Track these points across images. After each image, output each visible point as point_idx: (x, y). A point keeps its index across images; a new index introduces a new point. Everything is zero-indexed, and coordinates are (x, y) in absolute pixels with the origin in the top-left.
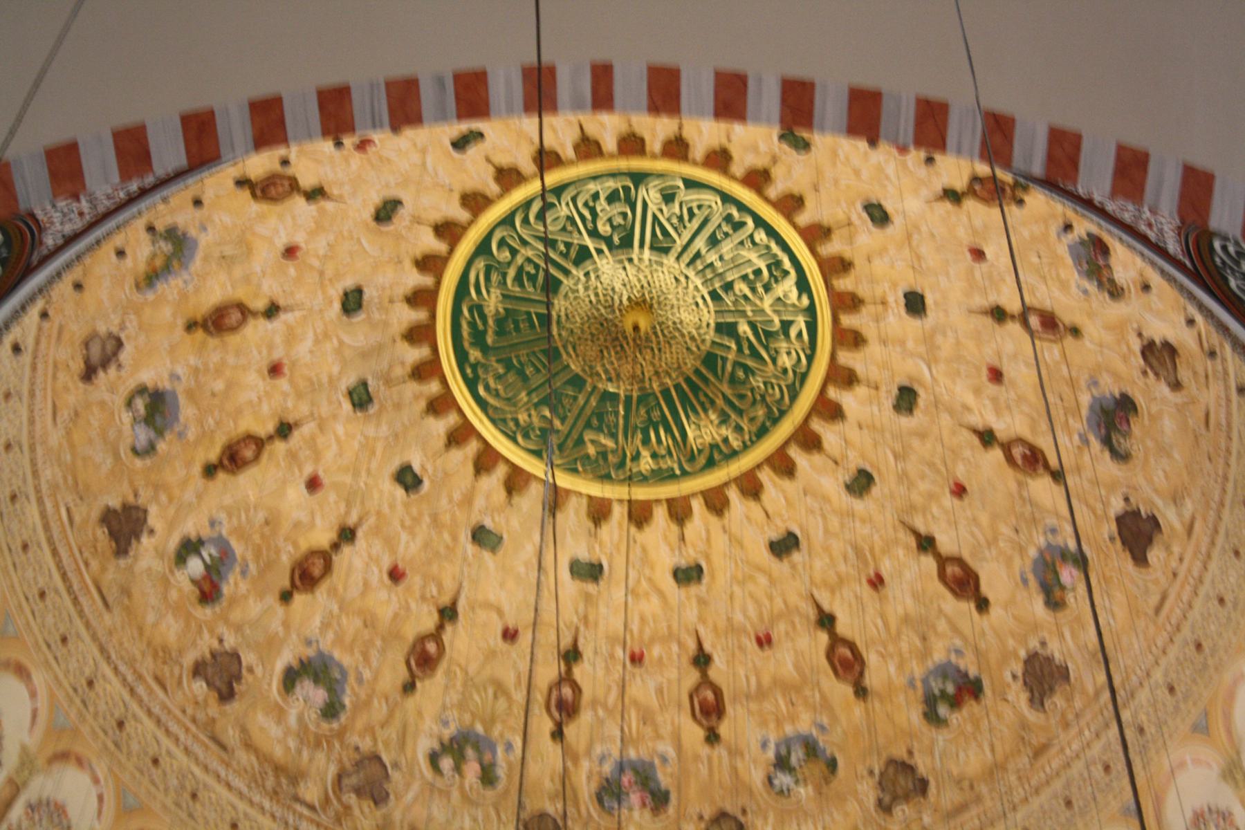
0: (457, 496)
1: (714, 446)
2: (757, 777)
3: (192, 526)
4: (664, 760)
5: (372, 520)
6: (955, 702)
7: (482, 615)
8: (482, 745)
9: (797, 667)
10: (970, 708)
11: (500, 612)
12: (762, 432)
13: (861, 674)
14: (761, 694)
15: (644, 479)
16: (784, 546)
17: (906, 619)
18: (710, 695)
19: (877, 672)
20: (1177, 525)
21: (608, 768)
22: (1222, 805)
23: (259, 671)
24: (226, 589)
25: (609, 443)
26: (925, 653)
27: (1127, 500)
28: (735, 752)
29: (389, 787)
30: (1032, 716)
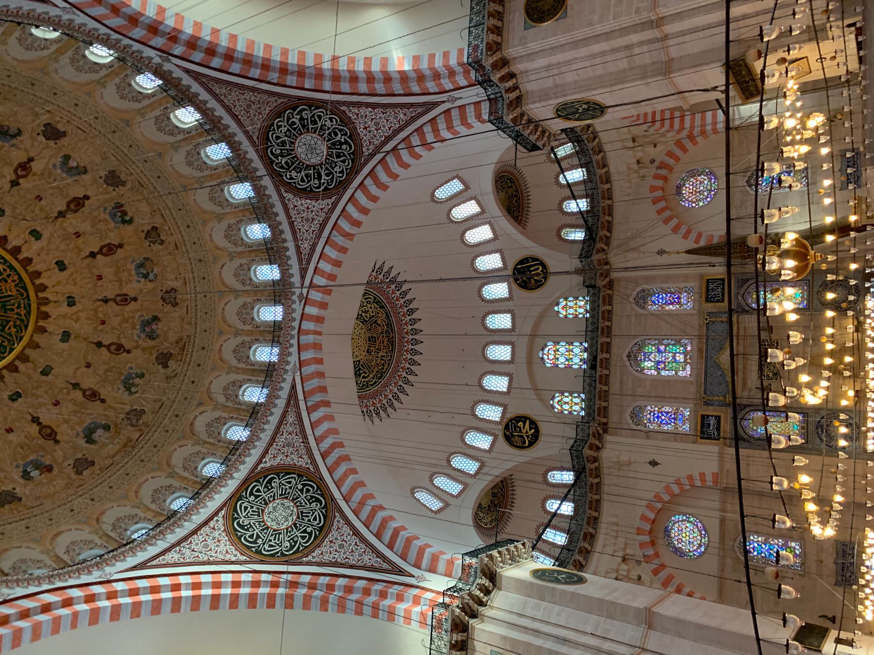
0: (26, 380)
1: (16, 286)
2: (150, 286)
3: (17, 475)
4: (142, 316)
5: (30, 410)
6: (125, 213)
7: (79, 373)
8: (129, 377)
9: (110, 267)
10: (126, 208)
11: (77, 369)
12: (11, 267)
13: (114, 245)
14: (120, 281)
15: (29, 313)
16: (61, 266)
17: (93, 226)
18: (119, 298)
19: (113, 238)
20: (48, 116)
21: (143, 336)
22: (115, 88)
23: (85, 452)
24: (48, 463)
25: (11, 323)
26: (106, 220)
27: (38, 134)
28: (141, 290)
29: (138, 408)
30: (129, 185)
